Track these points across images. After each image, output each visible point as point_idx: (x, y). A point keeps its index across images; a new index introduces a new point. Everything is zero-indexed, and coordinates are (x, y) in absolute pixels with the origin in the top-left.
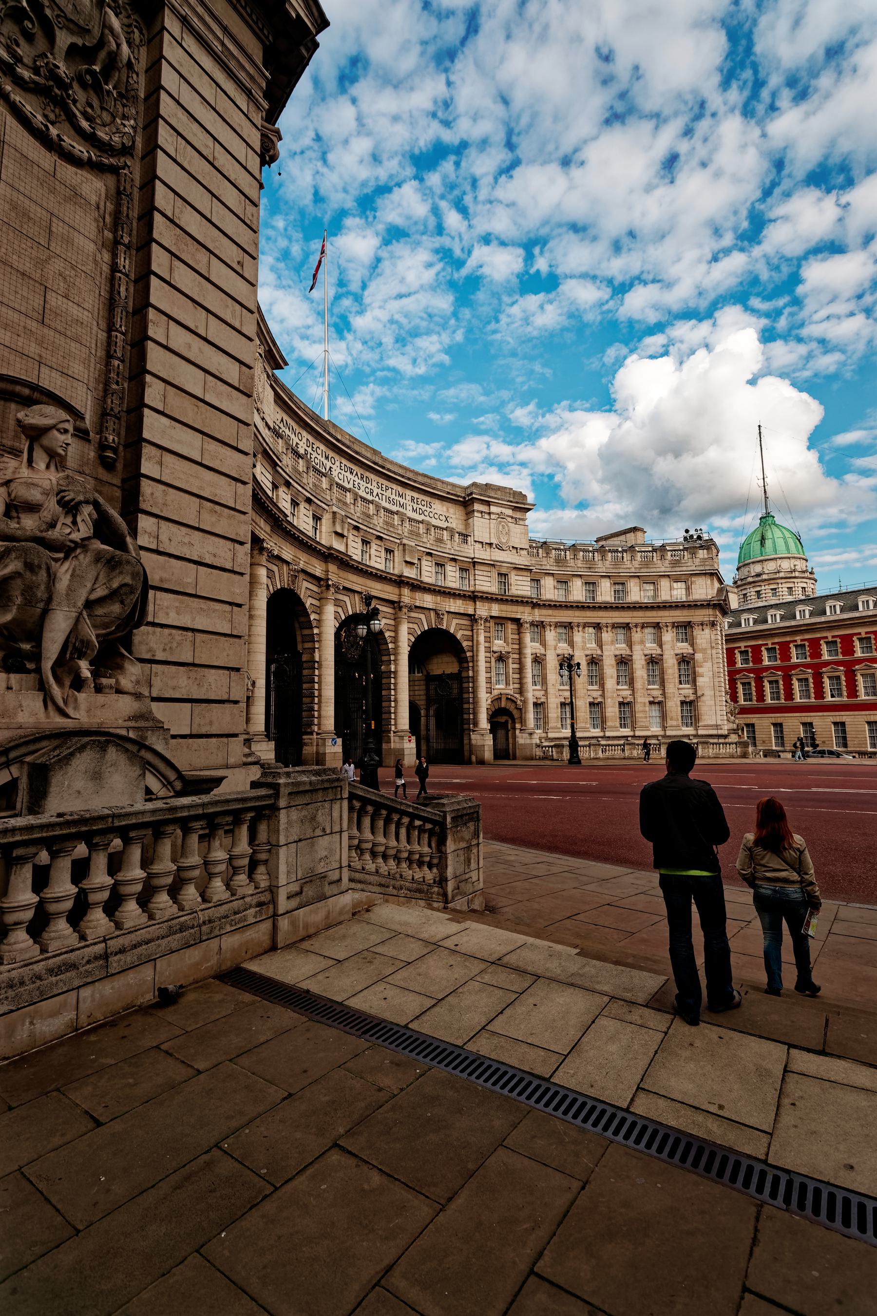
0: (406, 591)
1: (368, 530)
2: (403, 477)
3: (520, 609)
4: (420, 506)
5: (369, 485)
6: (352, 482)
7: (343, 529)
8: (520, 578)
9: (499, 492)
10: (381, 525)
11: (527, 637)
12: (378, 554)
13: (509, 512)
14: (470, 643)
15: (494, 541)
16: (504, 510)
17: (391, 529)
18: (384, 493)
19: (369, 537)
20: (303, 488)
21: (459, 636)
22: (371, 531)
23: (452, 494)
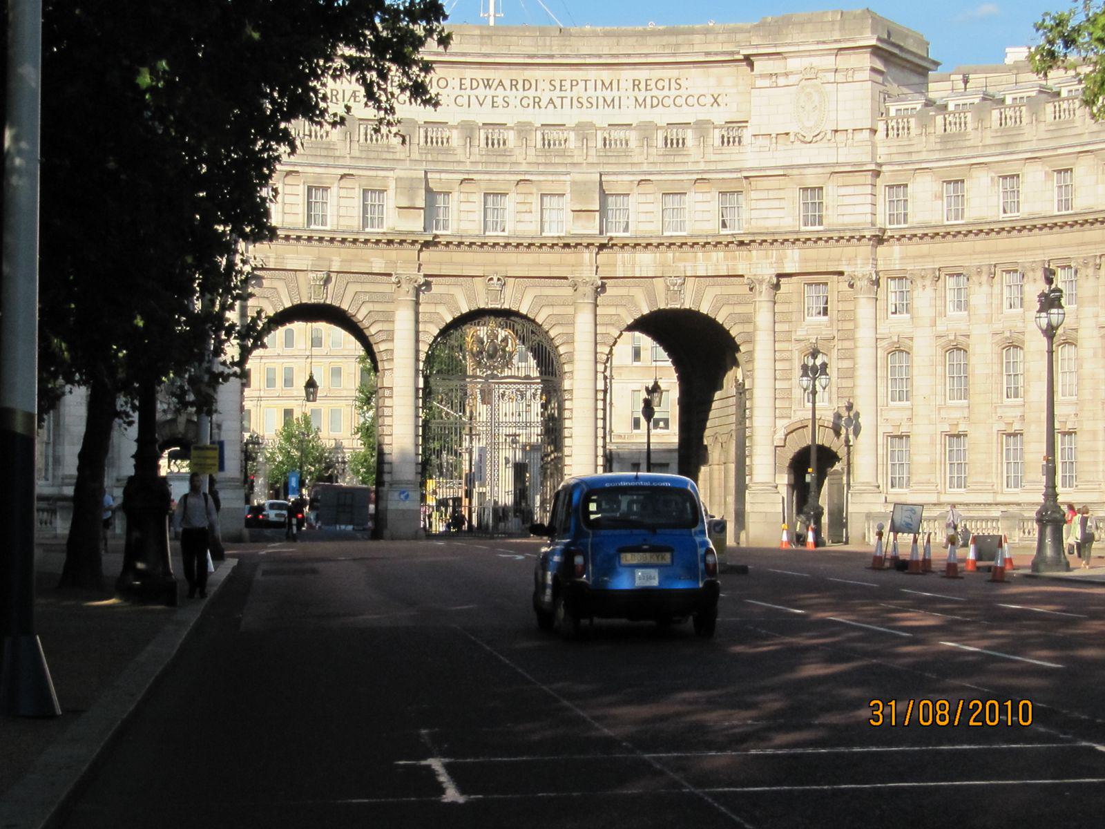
0: (587, 256)
1: (494, 177)
2: (600, 56)
3: (849, 251)
4: (655, 92)
5: (531, 93)
6: (489, 100)
7: (412, 199)
8: (850, 190)
9: (809, 27)
10: (531, 159)
11: (864, 309)
12: (524, 208)
13: (829, 62)
14: (748, 328)
15: (792, 129)
16: (817, 62)
17: (557, 160)
18: (568, 94)
19: (500, 188)
20: (327, 166)
21: (720, 320)
22: (501, 177)
23: (716, 54)
